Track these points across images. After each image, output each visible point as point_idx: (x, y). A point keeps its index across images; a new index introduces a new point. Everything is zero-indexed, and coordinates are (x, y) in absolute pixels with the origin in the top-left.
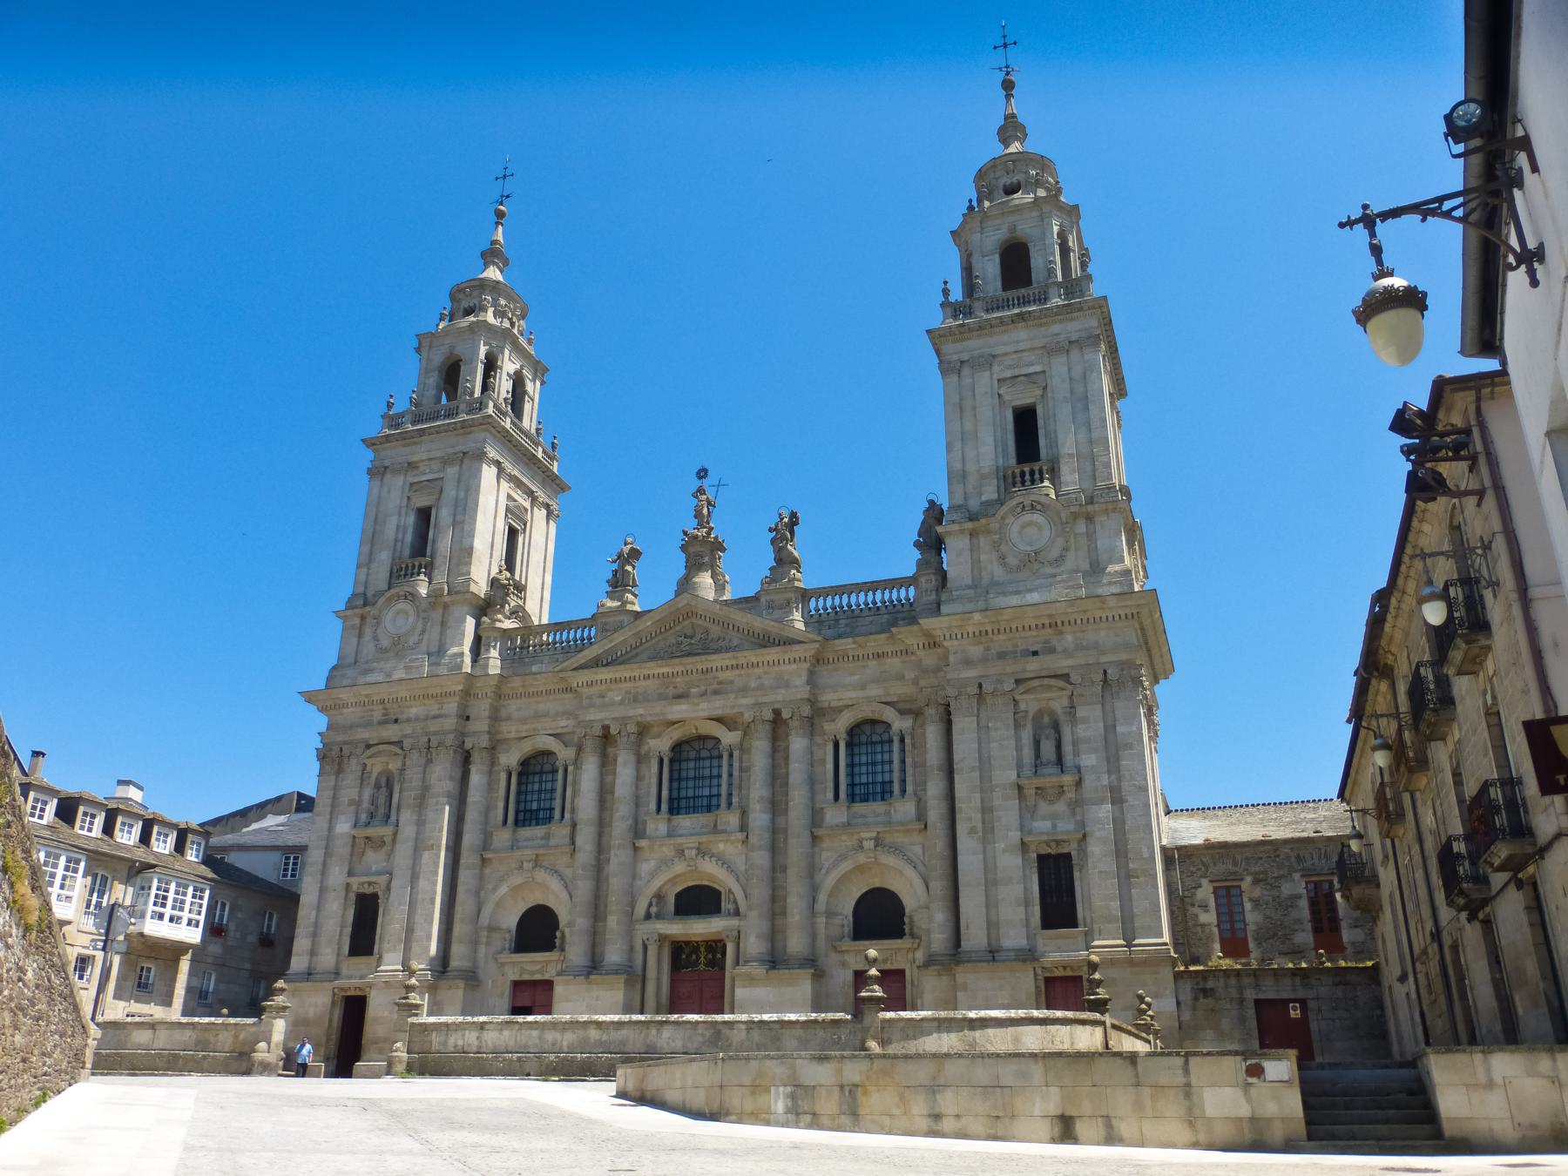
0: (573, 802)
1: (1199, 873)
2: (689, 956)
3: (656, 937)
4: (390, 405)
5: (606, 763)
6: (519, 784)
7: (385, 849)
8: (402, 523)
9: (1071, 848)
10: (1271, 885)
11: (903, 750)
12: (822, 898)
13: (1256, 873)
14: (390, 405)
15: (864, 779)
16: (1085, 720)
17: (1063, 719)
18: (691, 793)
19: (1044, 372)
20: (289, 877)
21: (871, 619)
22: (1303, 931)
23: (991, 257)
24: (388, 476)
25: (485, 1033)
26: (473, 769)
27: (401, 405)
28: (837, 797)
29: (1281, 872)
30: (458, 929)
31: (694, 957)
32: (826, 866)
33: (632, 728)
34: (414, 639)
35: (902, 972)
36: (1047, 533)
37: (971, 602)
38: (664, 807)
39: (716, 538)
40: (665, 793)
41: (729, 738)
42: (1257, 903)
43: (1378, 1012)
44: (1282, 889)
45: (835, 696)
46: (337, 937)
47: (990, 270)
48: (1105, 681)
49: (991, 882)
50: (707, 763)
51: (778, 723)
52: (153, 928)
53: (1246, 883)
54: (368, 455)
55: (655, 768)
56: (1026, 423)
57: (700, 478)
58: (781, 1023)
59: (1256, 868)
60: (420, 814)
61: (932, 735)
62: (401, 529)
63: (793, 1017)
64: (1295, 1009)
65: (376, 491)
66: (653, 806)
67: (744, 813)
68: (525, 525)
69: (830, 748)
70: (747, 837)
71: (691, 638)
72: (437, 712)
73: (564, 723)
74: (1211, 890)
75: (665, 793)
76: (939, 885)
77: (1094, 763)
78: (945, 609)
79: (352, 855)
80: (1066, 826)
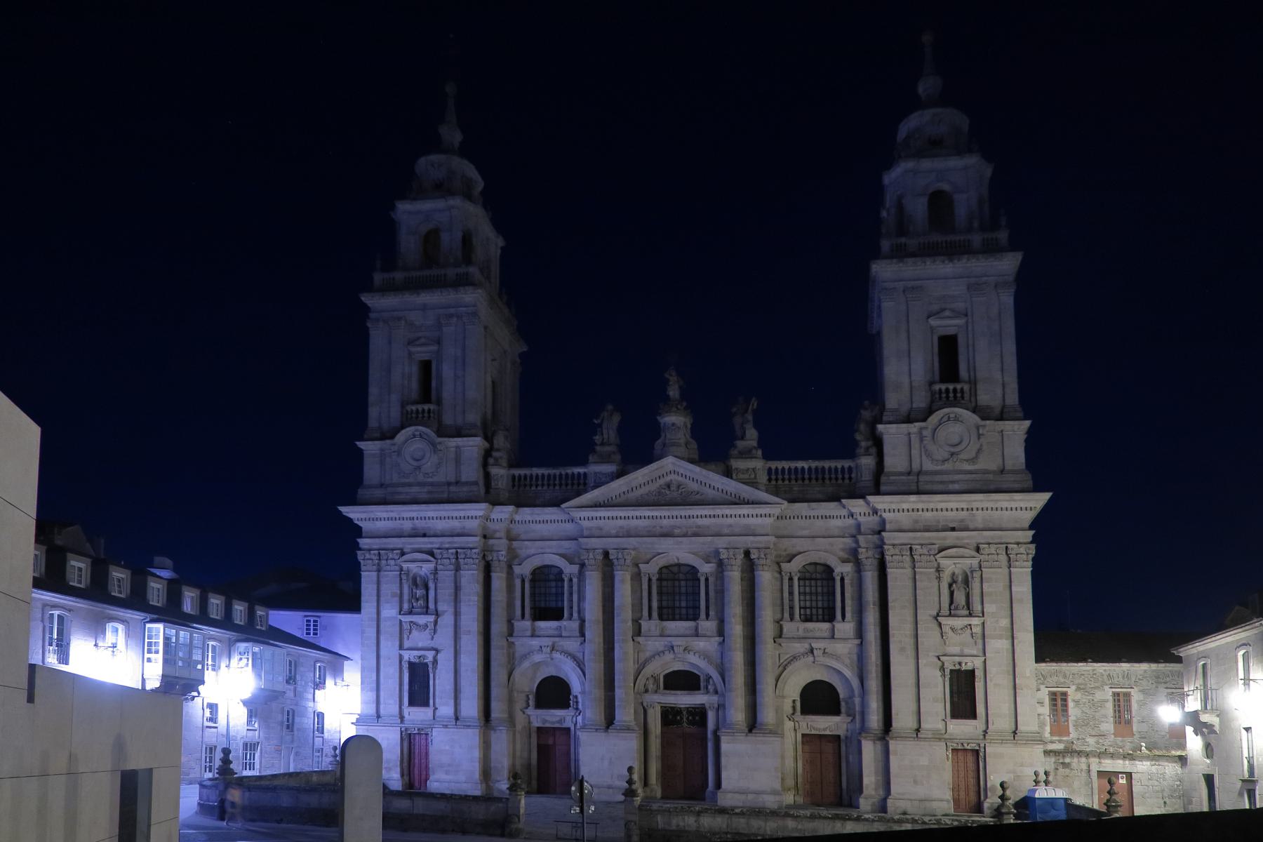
0: (579, 606)
6: (533, 587)
7: (427, 630)
10: (1088, 692)
13: (1079, 684)
20: (312, 635)
22: (1107, 722)
25: (701, 818)
29: (1096, 685)
38: (655, 614)
42: (1077, 702)
44: (1096, 695)
53: (1071, 691)
64: (1122, 778)
67: (721, 622)
70: (724, 640)
75: (655, 604)
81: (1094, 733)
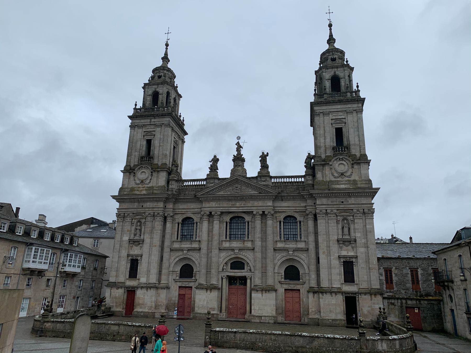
1: (380, 265)
2: (234, 281)
3: (226, 276)
4: (136, 105)
5: (210, 223)
8: (142, 144)
9: (354, 260)
10: (400, 270)
11: (300, 225)
12: (276, 268)
13: (396, 266)
14: (136, 105)
15: (287, 233)
16: (357, 223)
17: (350, 222)
18: (235, 233)
19: (345, 118)
20: (96, 247)
21: (291, 186)
22: (409, 283)
23: (329, 81)
24: (136, 129)
26: (167, 223)
27: (140, 105)
28: (280, 237)
30: (164, 271)
31: (235, 282)
32: (278, 258)
33: (219, 213)
34: (148, 181)
35: (299, 290)
36: (347, 167)
37: (323, 185)
38: (228, 237)
39: (244, 157)
40: (228, 233)
41: (247, 218)
43: (440, 312)
44: (403, 271)
45: (280, 208)
46: (125, 272)
47: (328, 84)
48: (364, 212)
49: (330, 267)
50: (240, 224)
51: (263, 215)
52: (68, 269)
53: (393, 269)
54: (130, 121)
55: (225, 226)
56: (339, 133)
57: (238, 139)
58: (334, 338)
59: (397, 265)
60: (151, 236)
61: (311, 223)
62: (142, 146)
63: (338, 337)
65: (132, 133)
66: (225, 237)
68: (177, 146)
69: (278, 223)
71: (237, 188)
72: (156, 204)
73: (196, 210)
74: (383, 270)
75: (228, 233)
76: (313, 267)
77: (360, 236)
78: (315, 187)
79: (129, 247)
80: (351, 254)
81: (404, 288)
